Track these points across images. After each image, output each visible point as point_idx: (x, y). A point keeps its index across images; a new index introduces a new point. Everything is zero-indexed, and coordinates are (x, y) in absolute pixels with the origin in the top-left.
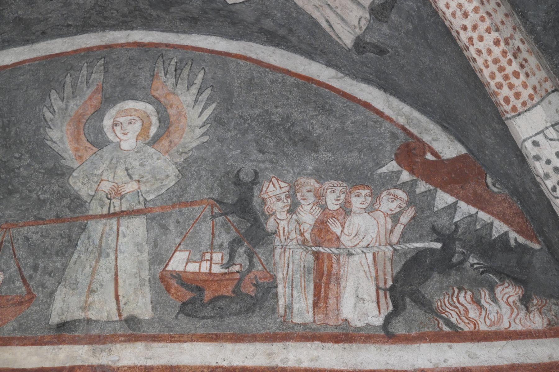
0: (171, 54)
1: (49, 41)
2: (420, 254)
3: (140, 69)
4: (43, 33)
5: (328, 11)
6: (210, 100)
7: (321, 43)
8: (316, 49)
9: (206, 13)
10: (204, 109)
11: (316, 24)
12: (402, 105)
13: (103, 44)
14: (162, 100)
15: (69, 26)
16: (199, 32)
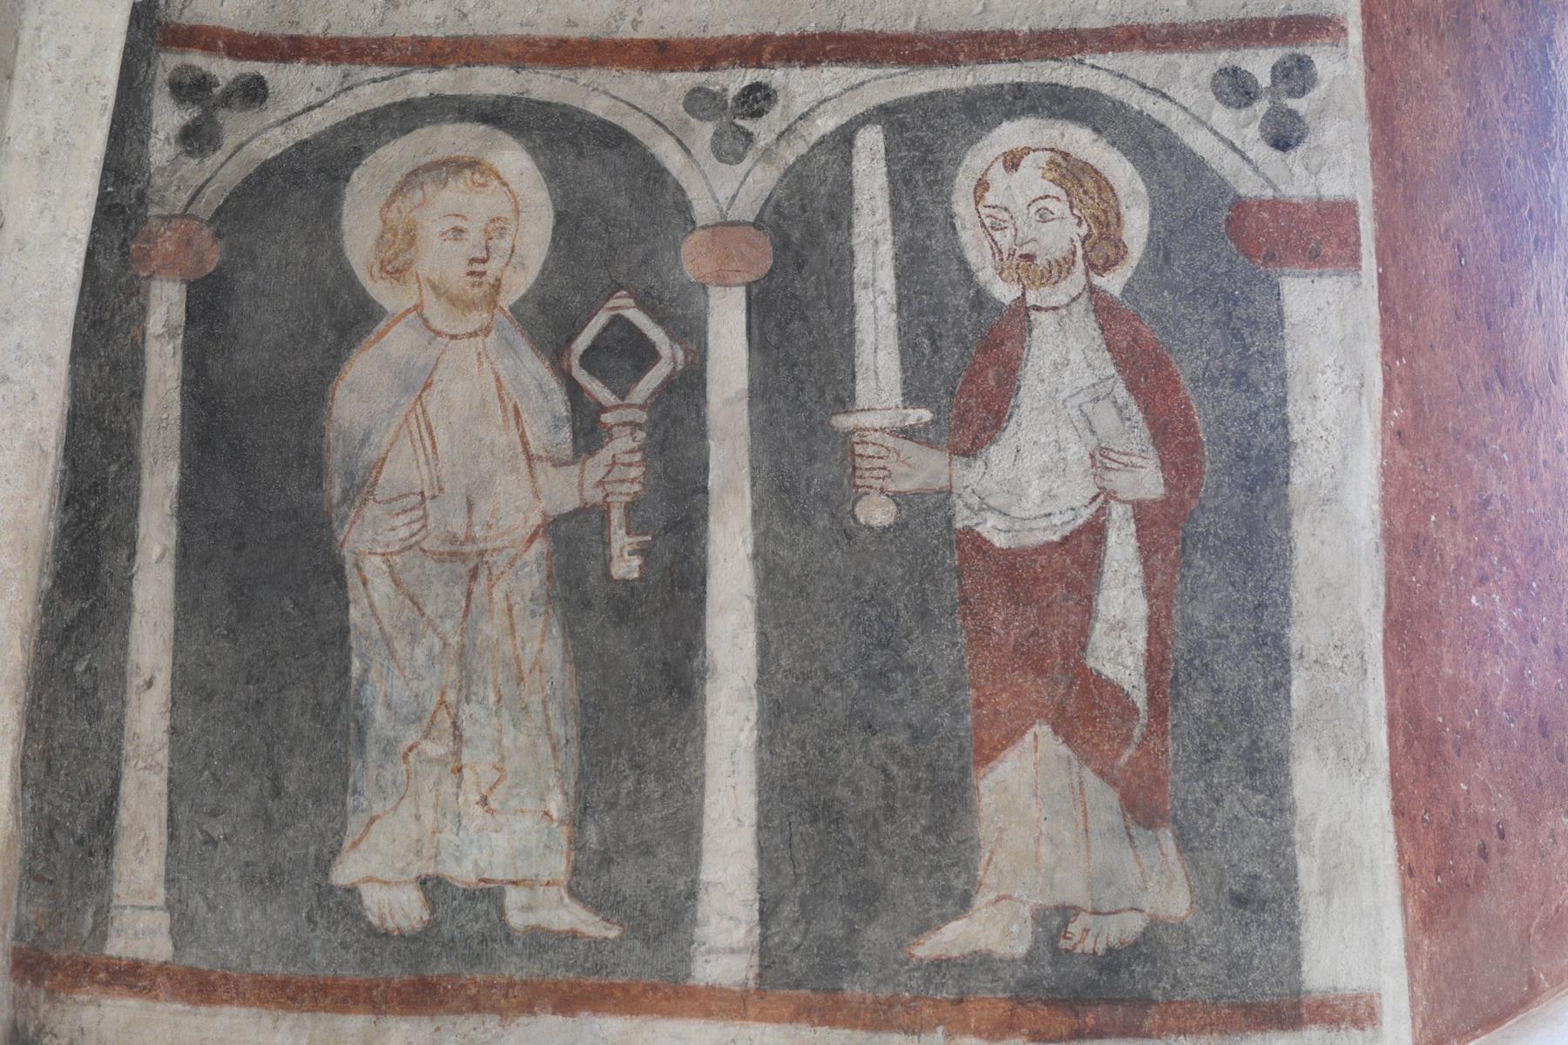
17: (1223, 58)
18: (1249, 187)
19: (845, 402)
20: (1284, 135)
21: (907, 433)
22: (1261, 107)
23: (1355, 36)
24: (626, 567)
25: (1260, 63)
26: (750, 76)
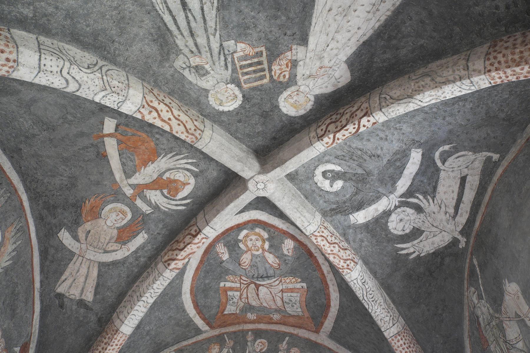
0: (23, 220)
1: (7, 160)
3: (13, 215)
4: (12, 157)
5: (71, 280)
6: (12, 258)
7: (52, 277)
8: (47, 274)
9: (48, 225)
10: (8, 260)
11: (62, 274)
12: (38, 323)
13: (16, 186)
14: (5, 240)
15: (21, 168)
16: (35, 221)
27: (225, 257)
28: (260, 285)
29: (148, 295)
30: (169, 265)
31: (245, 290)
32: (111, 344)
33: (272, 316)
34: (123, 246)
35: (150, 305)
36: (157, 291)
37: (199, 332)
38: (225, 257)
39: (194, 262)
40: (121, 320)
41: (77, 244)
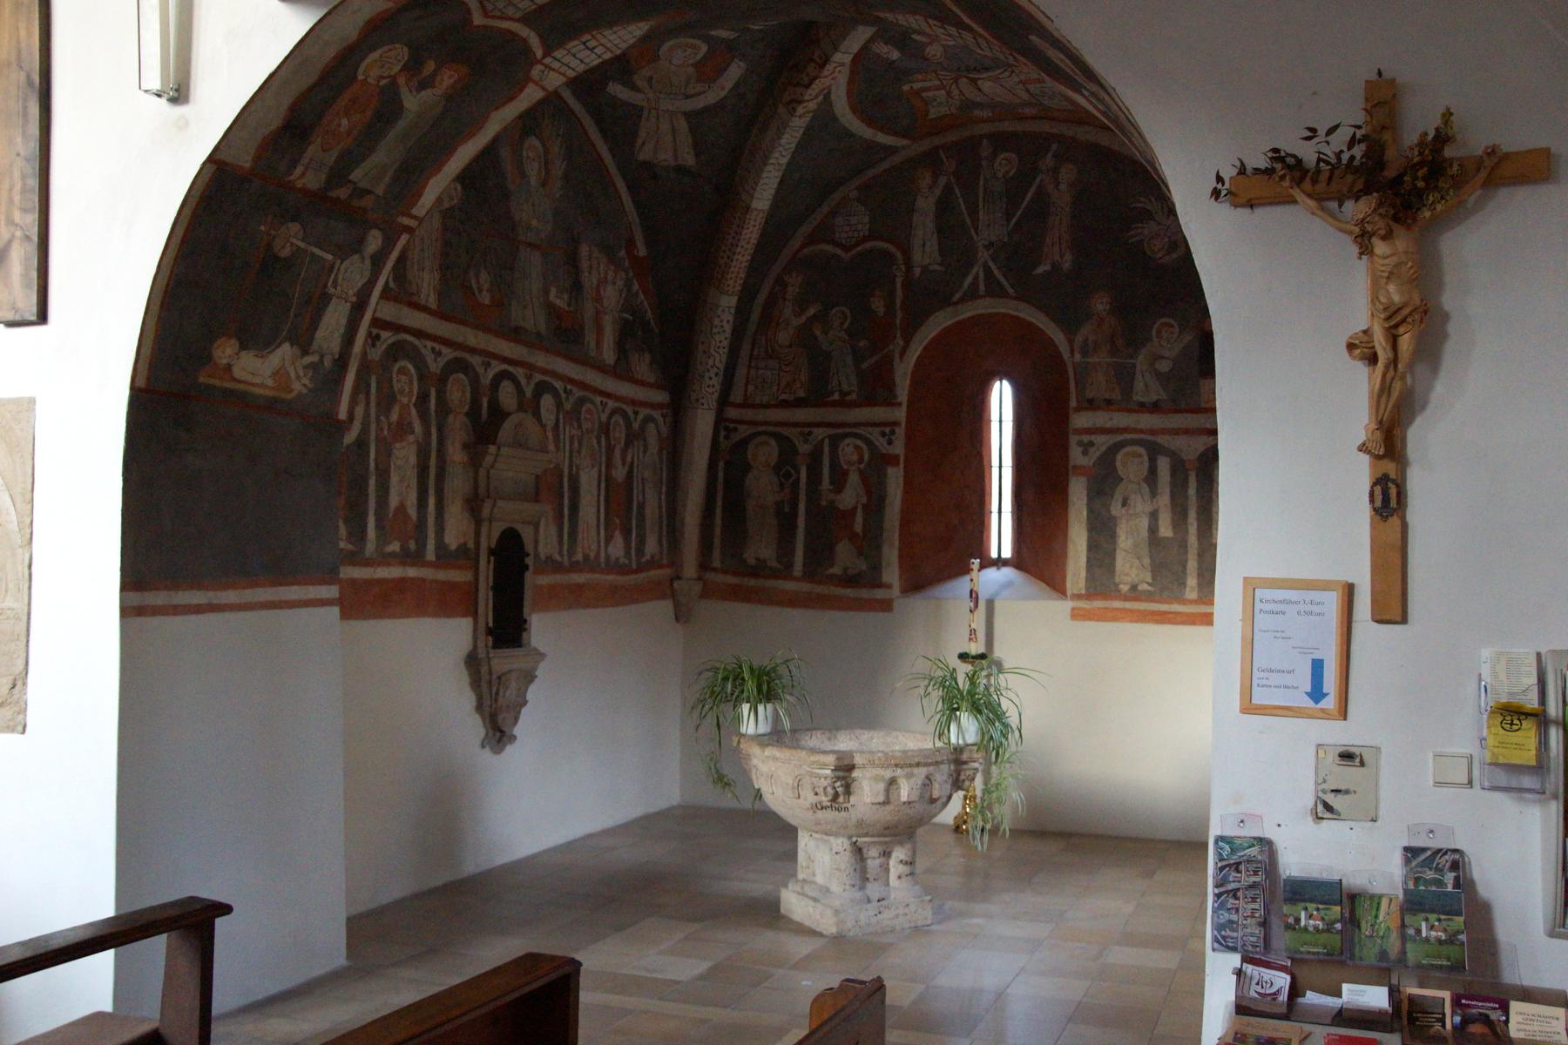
2: (627, 321)
17: (882, 429)
18: (884, 451)
19: (820, 484)
20: (890, 443)
21: (829, 490)
22: (887, 437)
23: (903, 425)
24: (787, 510)
25: (887, 430)
26: (808, 429)
27: (895, 55)
28: (979, 79)
29: (777, 155)
30: (794, 110)
31: (954, 86)
32: (745, 226)
33: (1020, 110)
34: (712, 85)
35: (784, 167)
36: (788, 146)
37: (891, 150)
38: (895, 55)
39: (842, 78)
40: (748, 192)
41: (641, 96)
